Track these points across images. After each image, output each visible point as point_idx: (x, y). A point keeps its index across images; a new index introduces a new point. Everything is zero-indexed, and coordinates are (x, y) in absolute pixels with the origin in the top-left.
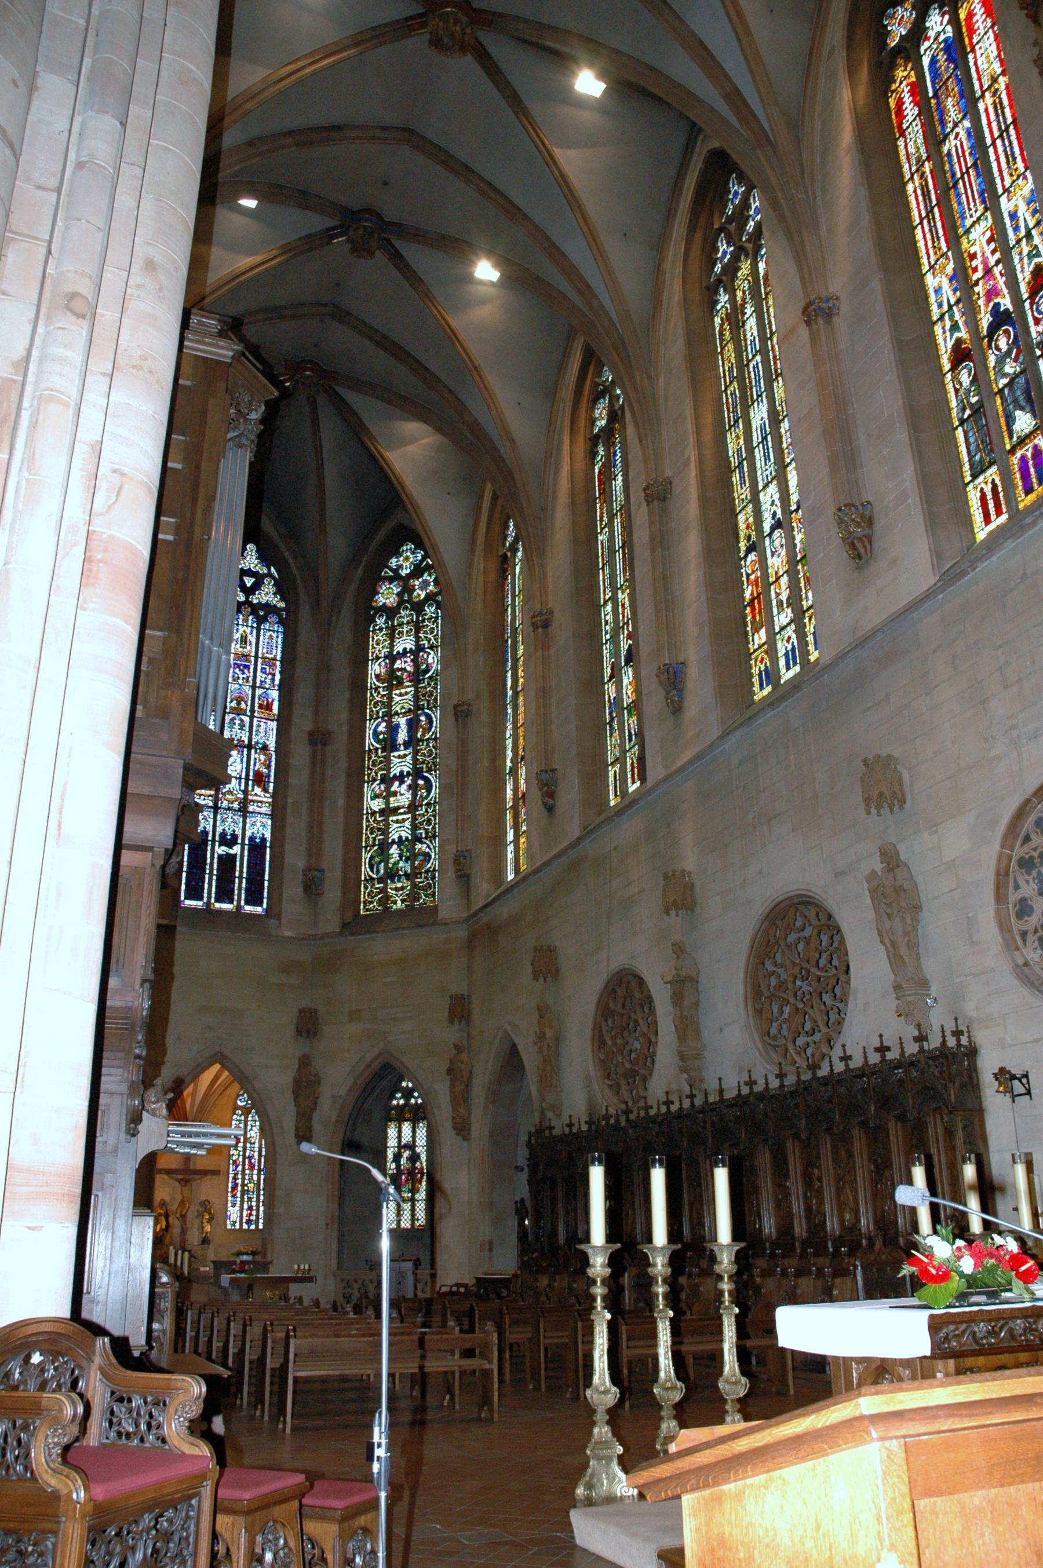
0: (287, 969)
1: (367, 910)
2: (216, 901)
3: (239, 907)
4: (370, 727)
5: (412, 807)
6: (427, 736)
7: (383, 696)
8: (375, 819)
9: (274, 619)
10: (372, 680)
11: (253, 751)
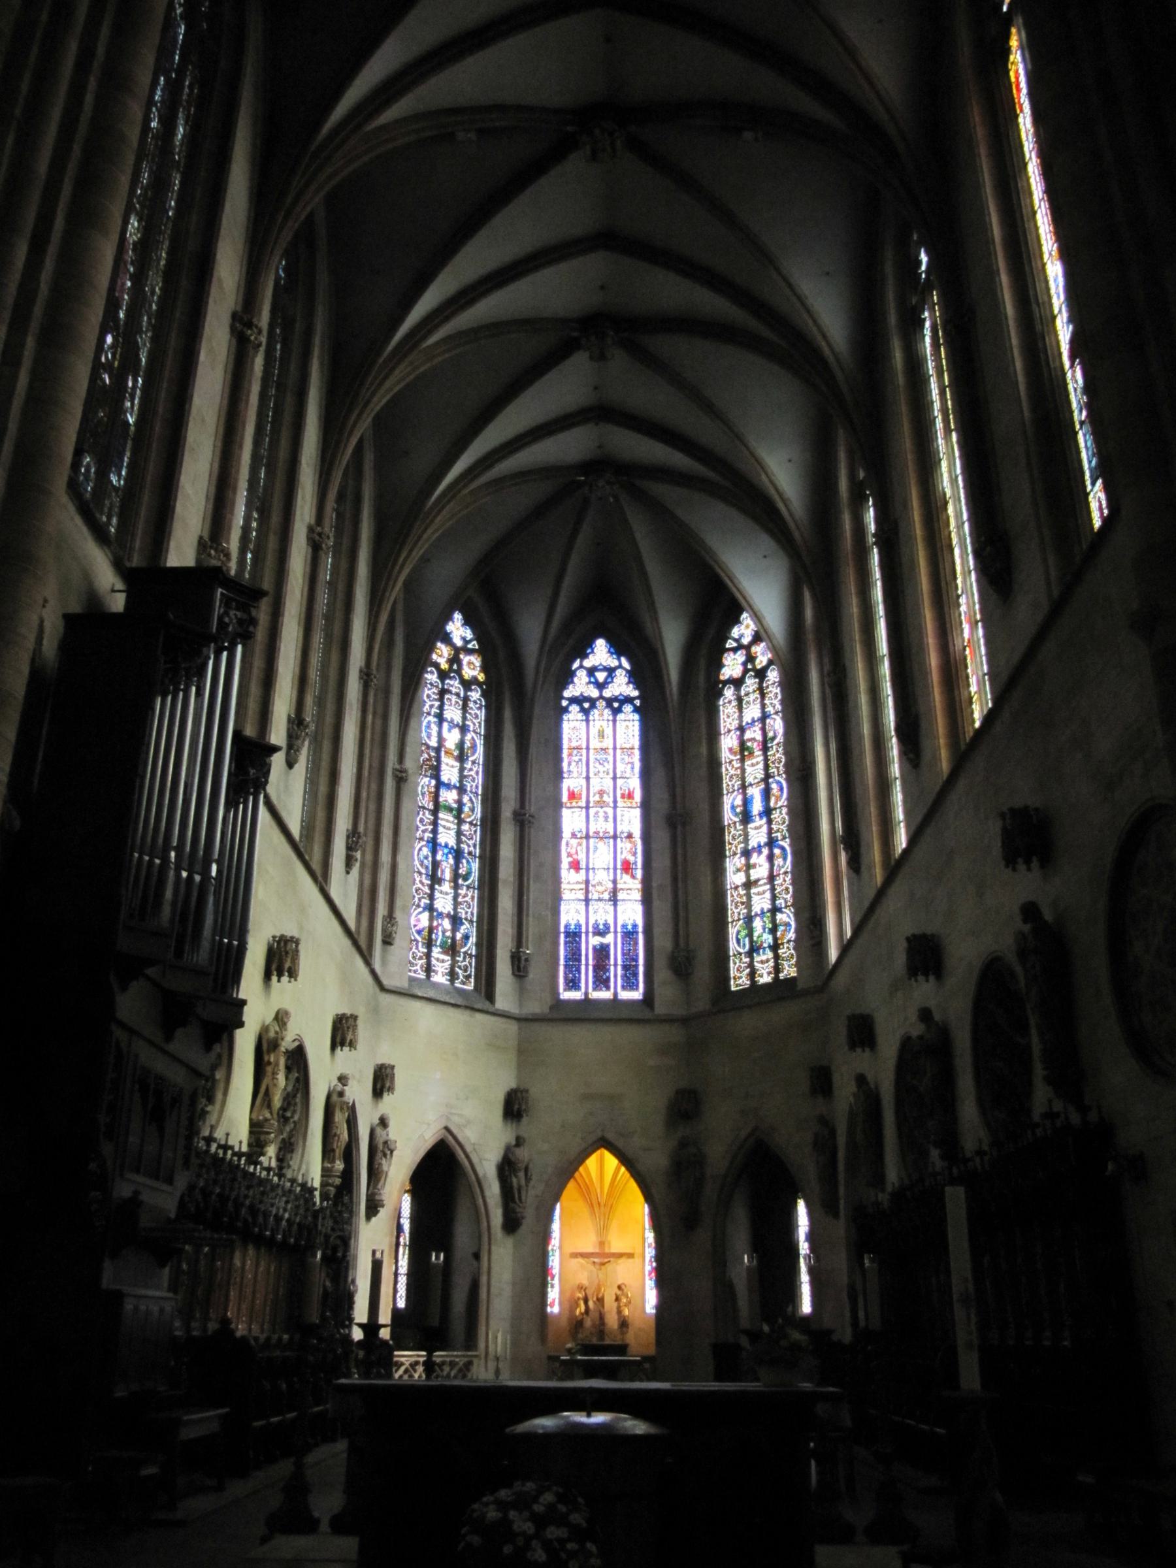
1: (737, 986)
2: (594, 989)
3: (615, 994)
4: (727, 801)
5: (772, 878)
6: (780, 804)
7: (736, 769)
8: (739, 894)
9: (628, 708)
10: (725, 755)
11: (619, 840)
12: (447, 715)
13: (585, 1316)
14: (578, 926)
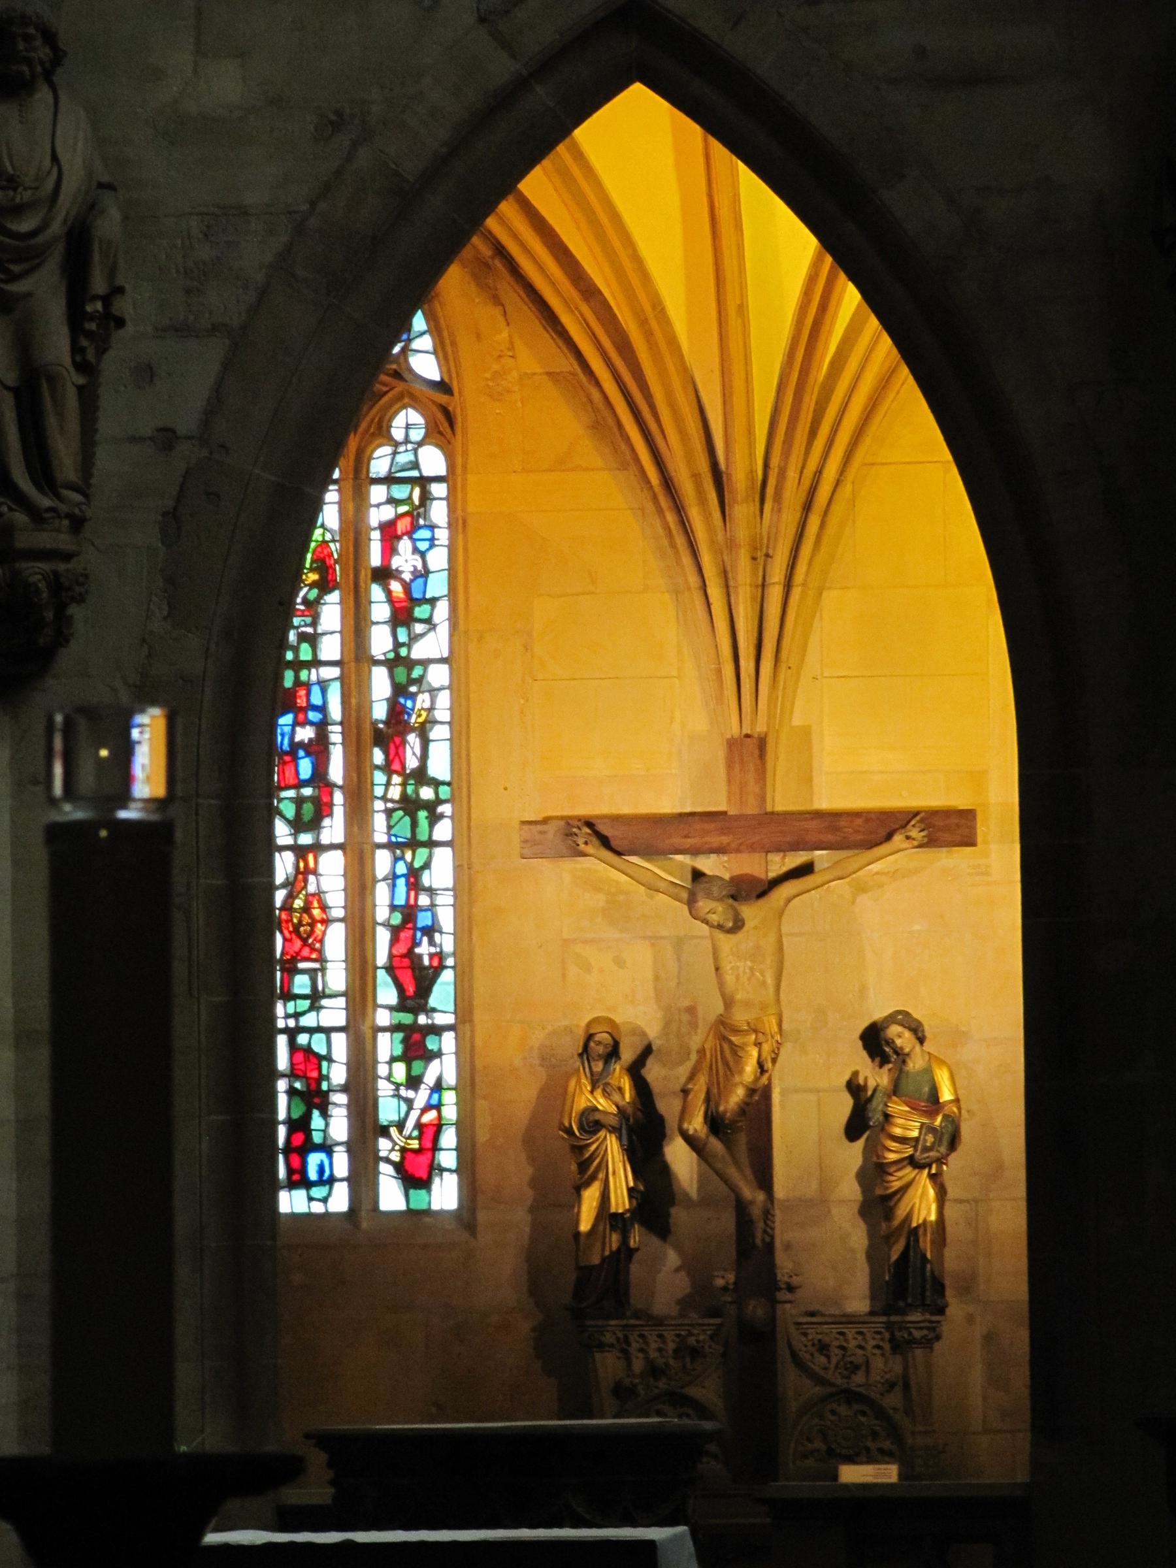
13: (636, 1237)
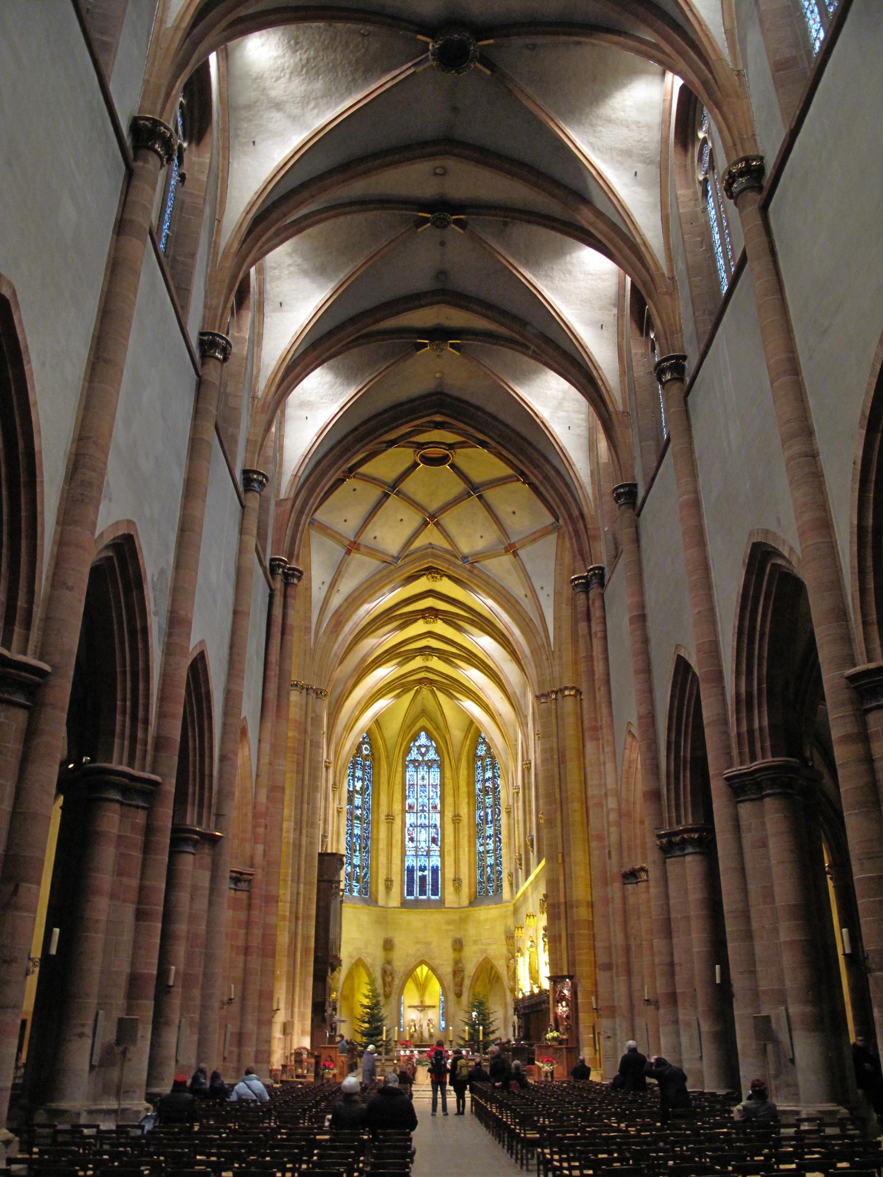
0: (449, 923)
3: (429, 898)
4: (478, 813)
10: (477, 791)
12: (357, 775)
14: (413, 867)
